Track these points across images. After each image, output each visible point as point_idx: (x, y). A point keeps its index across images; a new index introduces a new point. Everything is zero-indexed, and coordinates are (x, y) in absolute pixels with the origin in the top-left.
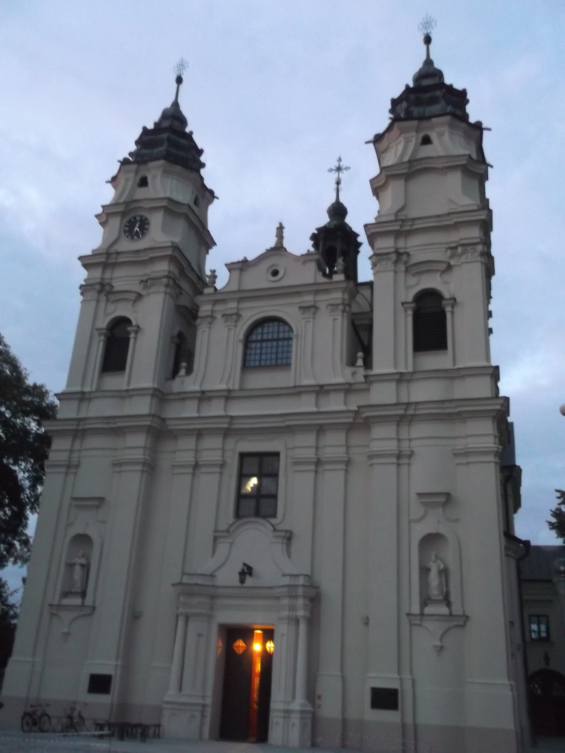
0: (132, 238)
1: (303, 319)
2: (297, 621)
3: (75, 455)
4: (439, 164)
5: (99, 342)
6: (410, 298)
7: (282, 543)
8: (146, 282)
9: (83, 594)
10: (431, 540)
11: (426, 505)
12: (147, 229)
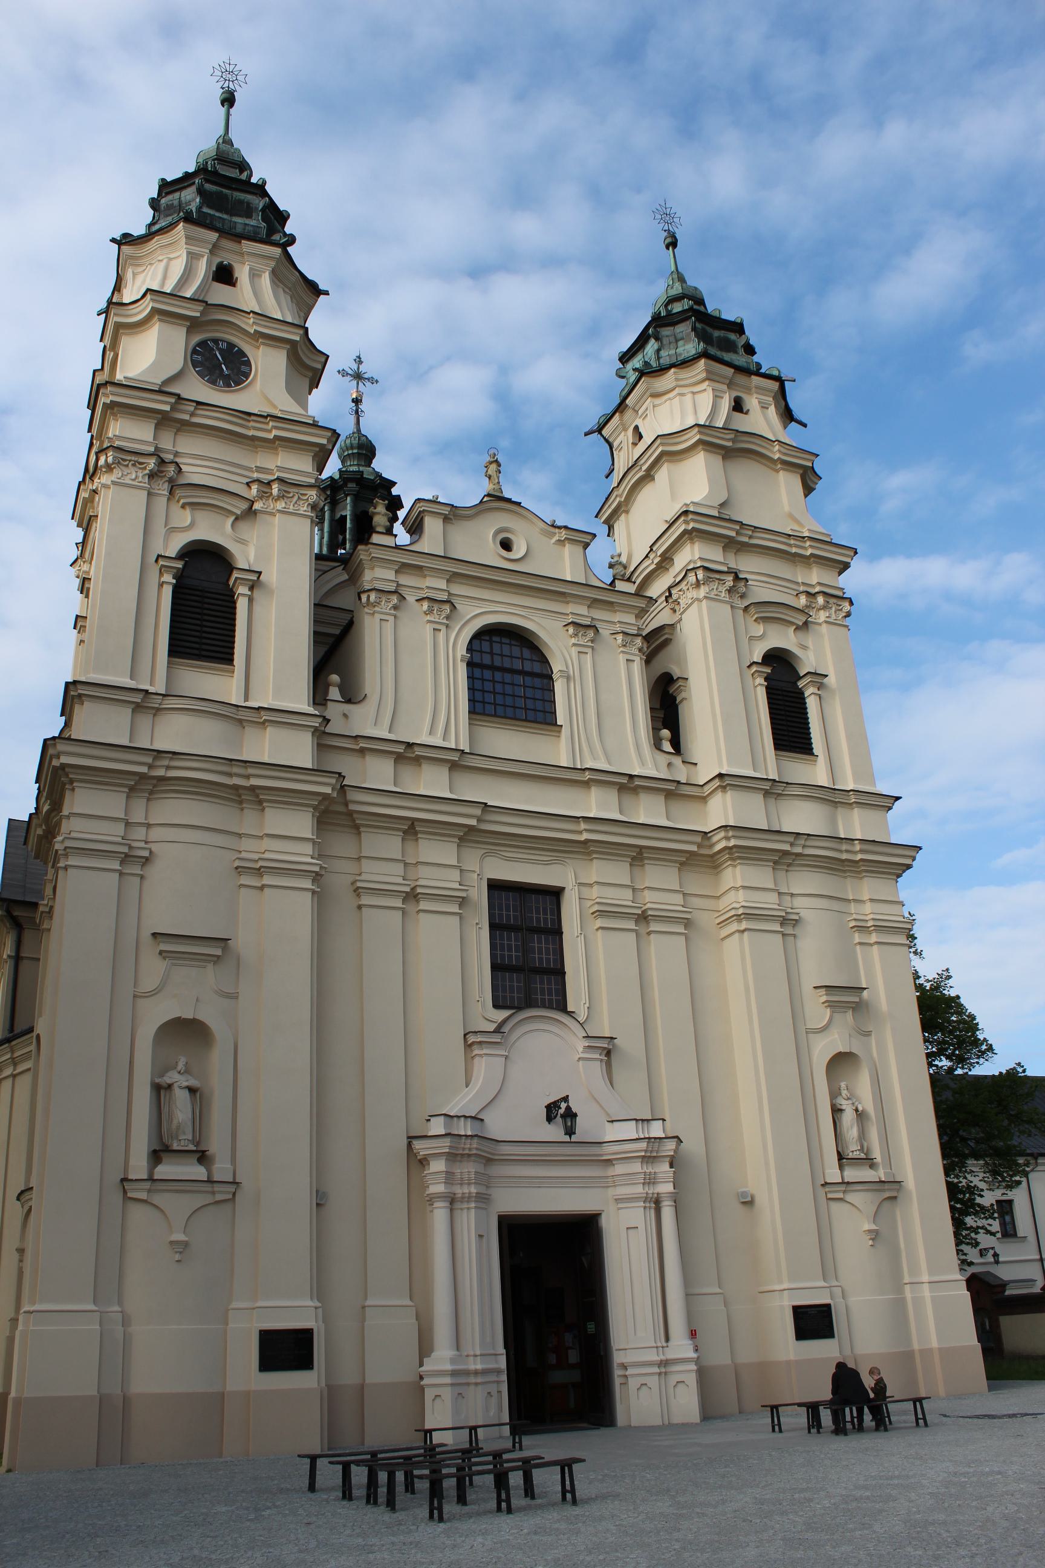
0: (213, 382)
1: (574, 645)
2: (657, 1203)
3: (140, 833)
4: (776, 453)
5: (161, 585)
6: (758, 657)
7: (601, 1060)
10: (841, 1062)
11: (830, 1004)
12: (247, 376)
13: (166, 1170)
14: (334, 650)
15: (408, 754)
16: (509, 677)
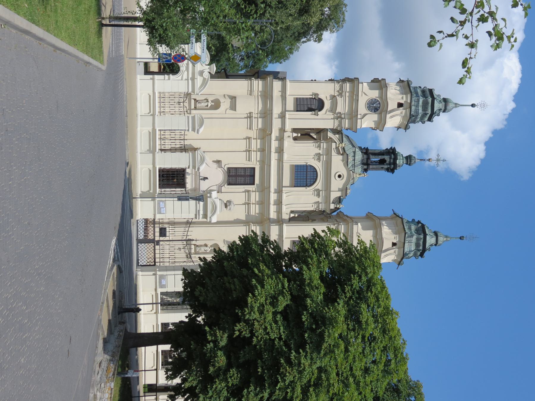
8: (339, 117)
9: (195, 108)
13: (193, 101)
14: (305, 134)
15: (280, 151)
16: (304, 176)
